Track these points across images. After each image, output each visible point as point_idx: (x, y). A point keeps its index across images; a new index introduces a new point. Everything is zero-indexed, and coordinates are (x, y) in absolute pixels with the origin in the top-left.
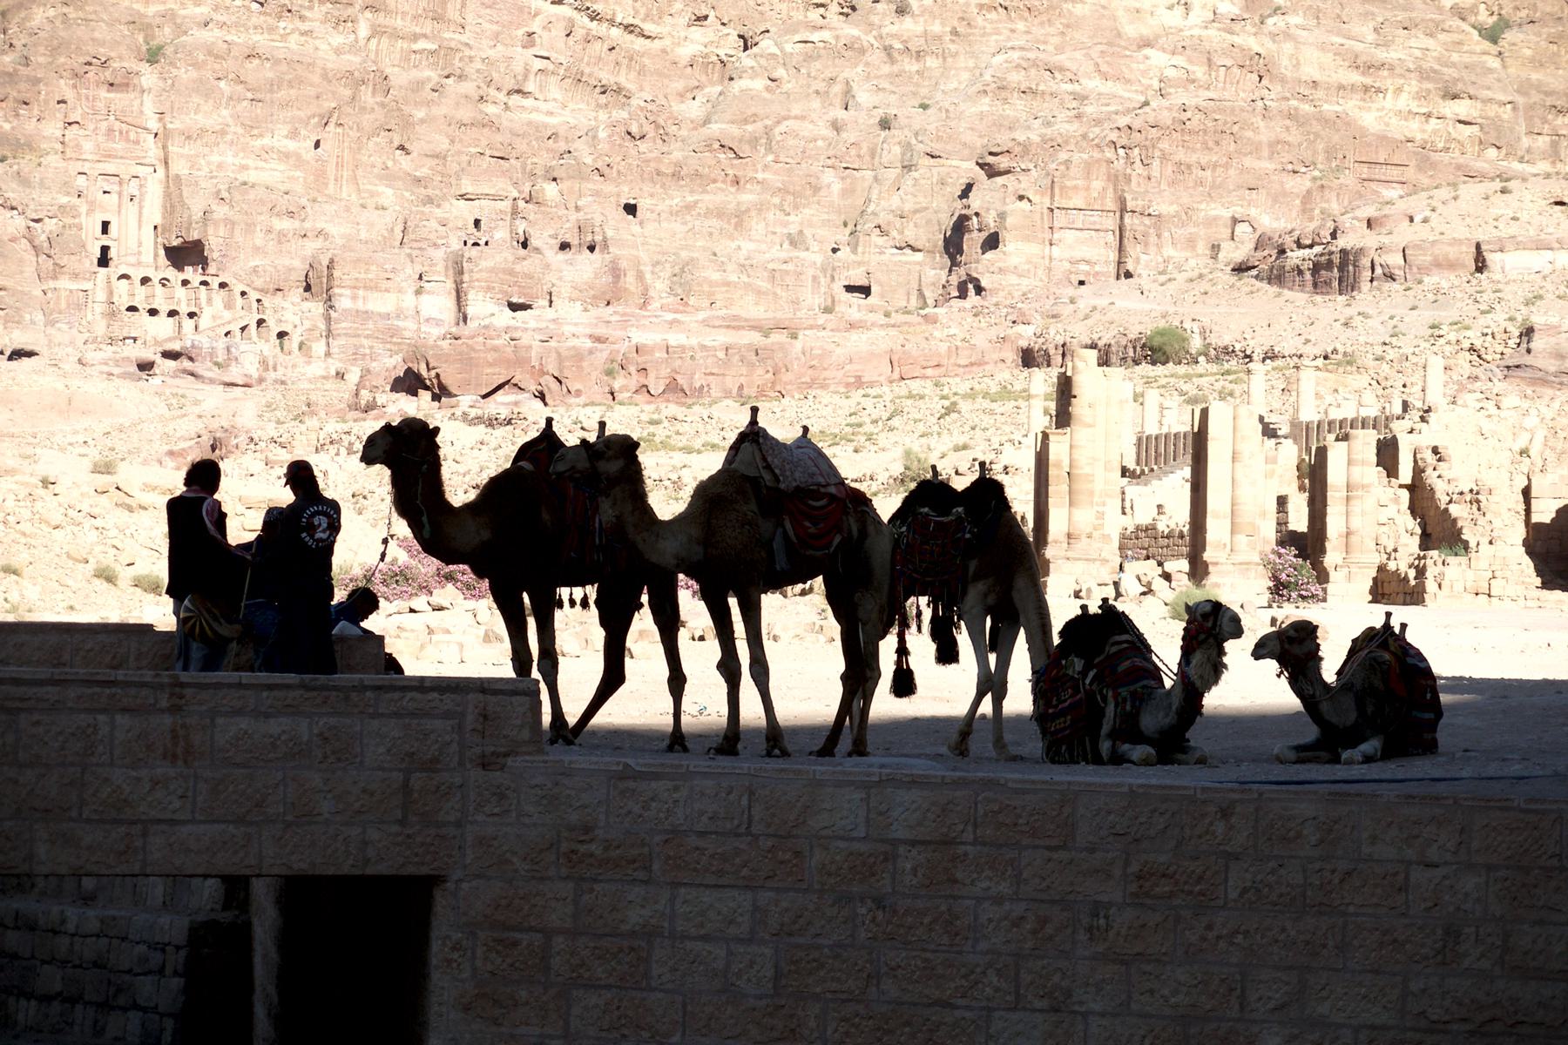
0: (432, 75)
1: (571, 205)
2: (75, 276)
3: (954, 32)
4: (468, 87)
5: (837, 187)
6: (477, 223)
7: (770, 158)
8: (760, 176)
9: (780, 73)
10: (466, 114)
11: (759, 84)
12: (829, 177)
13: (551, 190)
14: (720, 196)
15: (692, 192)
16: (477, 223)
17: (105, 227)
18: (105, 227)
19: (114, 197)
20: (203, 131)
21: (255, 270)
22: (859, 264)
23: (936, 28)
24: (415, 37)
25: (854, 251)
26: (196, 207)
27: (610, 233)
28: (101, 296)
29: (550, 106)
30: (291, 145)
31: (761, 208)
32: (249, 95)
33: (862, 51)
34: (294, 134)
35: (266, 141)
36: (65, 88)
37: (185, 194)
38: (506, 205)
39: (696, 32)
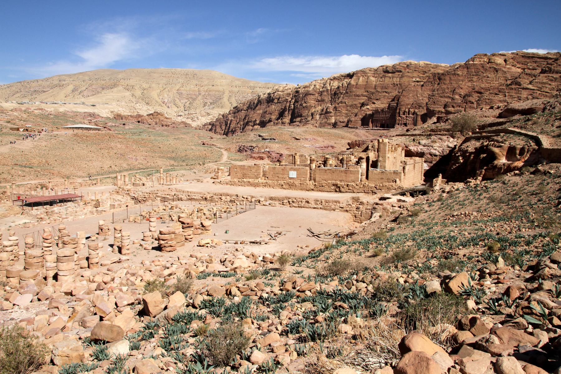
36: (465, 104)
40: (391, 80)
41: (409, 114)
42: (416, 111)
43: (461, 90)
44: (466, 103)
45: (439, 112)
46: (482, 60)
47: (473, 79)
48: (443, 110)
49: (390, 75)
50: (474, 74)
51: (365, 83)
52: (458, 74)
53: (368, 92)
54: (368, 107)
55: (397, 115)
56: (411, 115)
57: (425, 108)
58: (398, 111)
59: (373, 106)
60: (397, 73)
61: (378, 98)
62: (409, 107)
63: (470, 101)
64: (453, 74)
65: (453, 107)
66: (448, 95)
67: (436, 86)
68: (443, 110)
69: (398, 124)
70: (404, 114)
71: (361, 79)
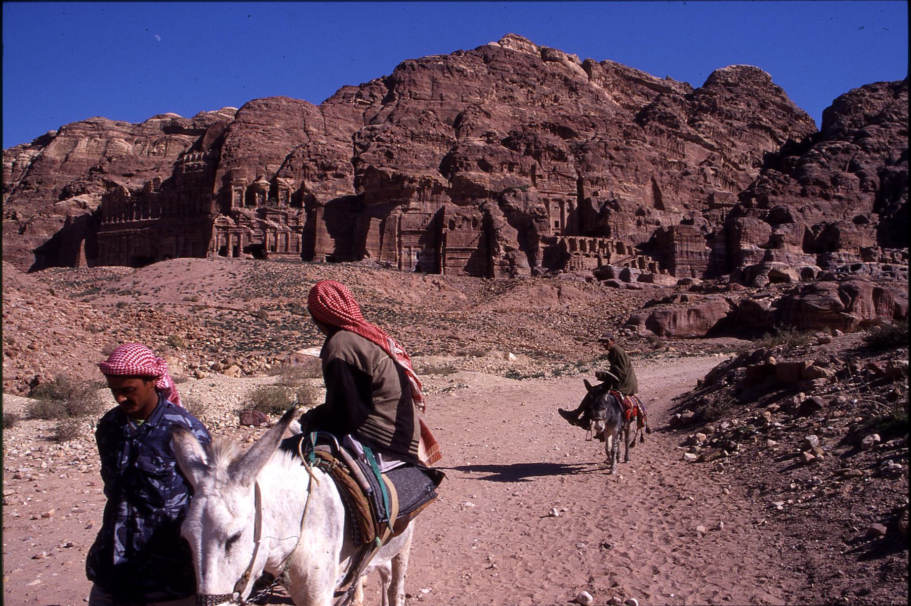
30: (635, 186)
36: (531, 160)
42: (309, 185)
43: (487, 121)
44: (537, 156)
45: (425, 183)
47: (516, 95)
48: (444, 181)
55: (214, 208)
57: (350, 177)
62: (274, 168)
65: (485, 166)
67: (378, 105)
68: (444, 181)
69: (224, 252)
70: (250, 202)
71: (83, 144)
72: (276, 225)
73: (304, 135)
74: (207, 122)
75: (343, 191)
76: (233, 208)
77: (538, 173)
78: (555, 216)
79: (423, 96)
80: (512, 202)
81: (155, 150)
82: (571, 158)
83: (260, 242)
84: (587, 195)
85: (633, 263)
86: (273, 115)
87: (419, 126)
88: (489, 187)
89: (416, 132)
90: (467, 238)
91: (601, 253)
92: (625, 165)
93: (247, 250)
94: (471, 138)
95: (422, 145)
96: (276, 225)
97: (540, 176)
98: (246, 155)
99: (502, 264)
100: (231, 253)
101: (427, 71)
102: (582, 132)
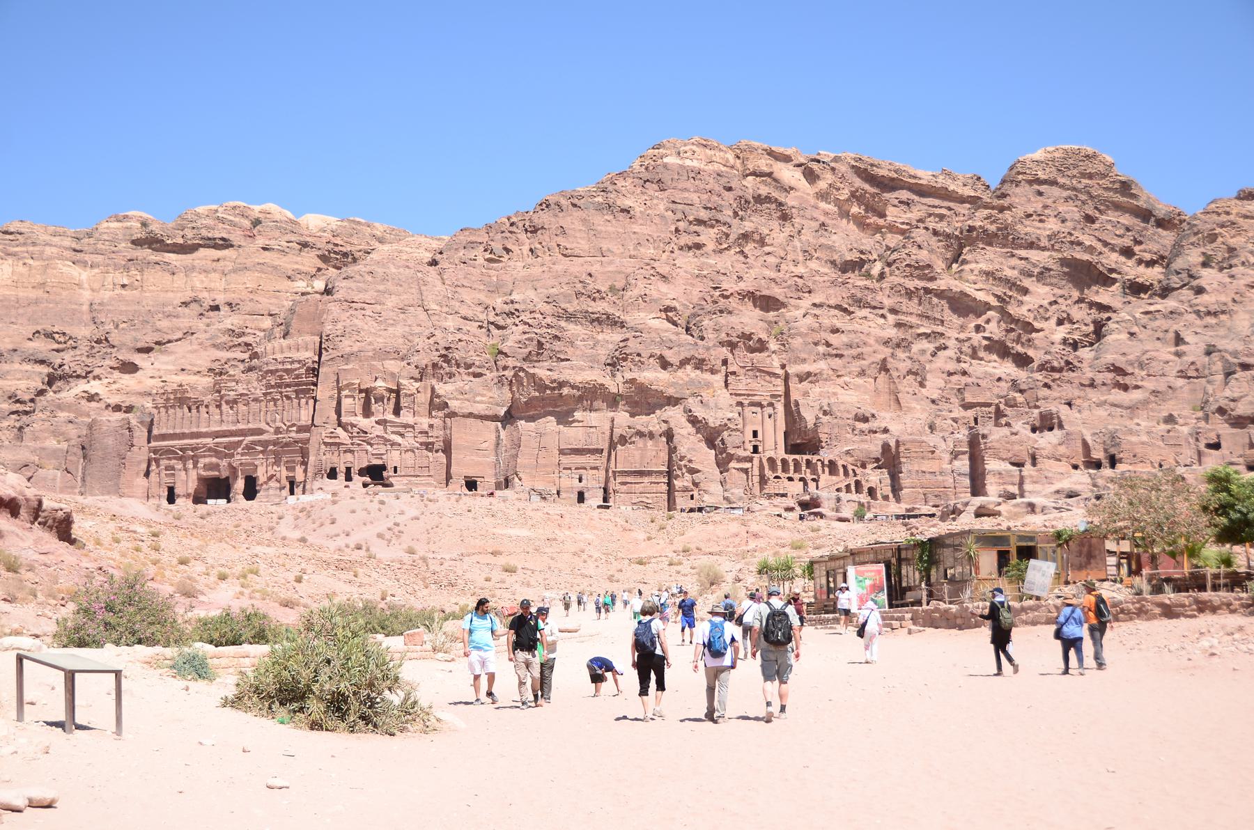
0: (931, 347)
1: (1032, 404)
2: (740, 460)
3: (1234, 301)
4: (950, 353)
5: (1186, 388)
6: (976, 420)
7: (1144, 373)
8: (1140, 383)
9: (1135, 329)
10: (952, 366)
11: (1124, 336)
12: (1181, 382)
13: (1020, 398)
14: (1118, 396)
15: (1103, 394)
16: (976, 420)
17: (755, 434)
18: (755, 434)
19: (759, 416)
20: (809, 374)
21: (848, 452)
22: (1212, 430)
23: (1223, 298)
24: (918, 326)
25: (1207, 422)
26: (809, 416)
27: (1063, 418)
28: (756, 472)
29: (993, 364)
30: (860, 381)
31: (1146, 402)
32: (835, 352)
33: (1180, 314)
34: (862, 373)
35: (846, 379)
36: (725, 352)
37: (802, 410)
38: (992, 409)
39: (1061, 328)
40: (179, 280)
41: (397, 411)
42: (441, 388)
43: (664, 288)
46: (718, 156)
47: (702, 239)
49: (171, 257)
50: (704, 215)
51: (33, 294)
52: (625, 211)
53: (50, 336)
54: (94, 387)
56: (406, 417)
58: (324, 391)
59: (127, 380)
60: (202, 252)
61: (148, 339)
63: (749, 337)
64: (599, 208)
65: (665, 364)
66: (600, 307)
69: (332, 474)
72: (398, 439)
73: (423, 316)
74: (204, 233)
75: (483, 395)
76: (344, 419)
77: (731, 369)
78: (753, 423)
79: (577, 252)
80: (699, 413)
81: (126, 282)
82: (773, 345)
83: (379, 462)
84: (794, 396)
85: (848, 487)
86: (381, 288)
87: (576, 302)
88: (671, 392)
89: (571, 310)
90: (642, 457)
91: (809, 477)
92: (845, 353)
93: (362, 472)
94: (642, 314)
95: (579, 327)
96: (398, 439)
97: (734, 373)
98: (355, 349)
99: (686, 490)
100: (341, 477)
101: (577, 213)
102: (792, 301)
